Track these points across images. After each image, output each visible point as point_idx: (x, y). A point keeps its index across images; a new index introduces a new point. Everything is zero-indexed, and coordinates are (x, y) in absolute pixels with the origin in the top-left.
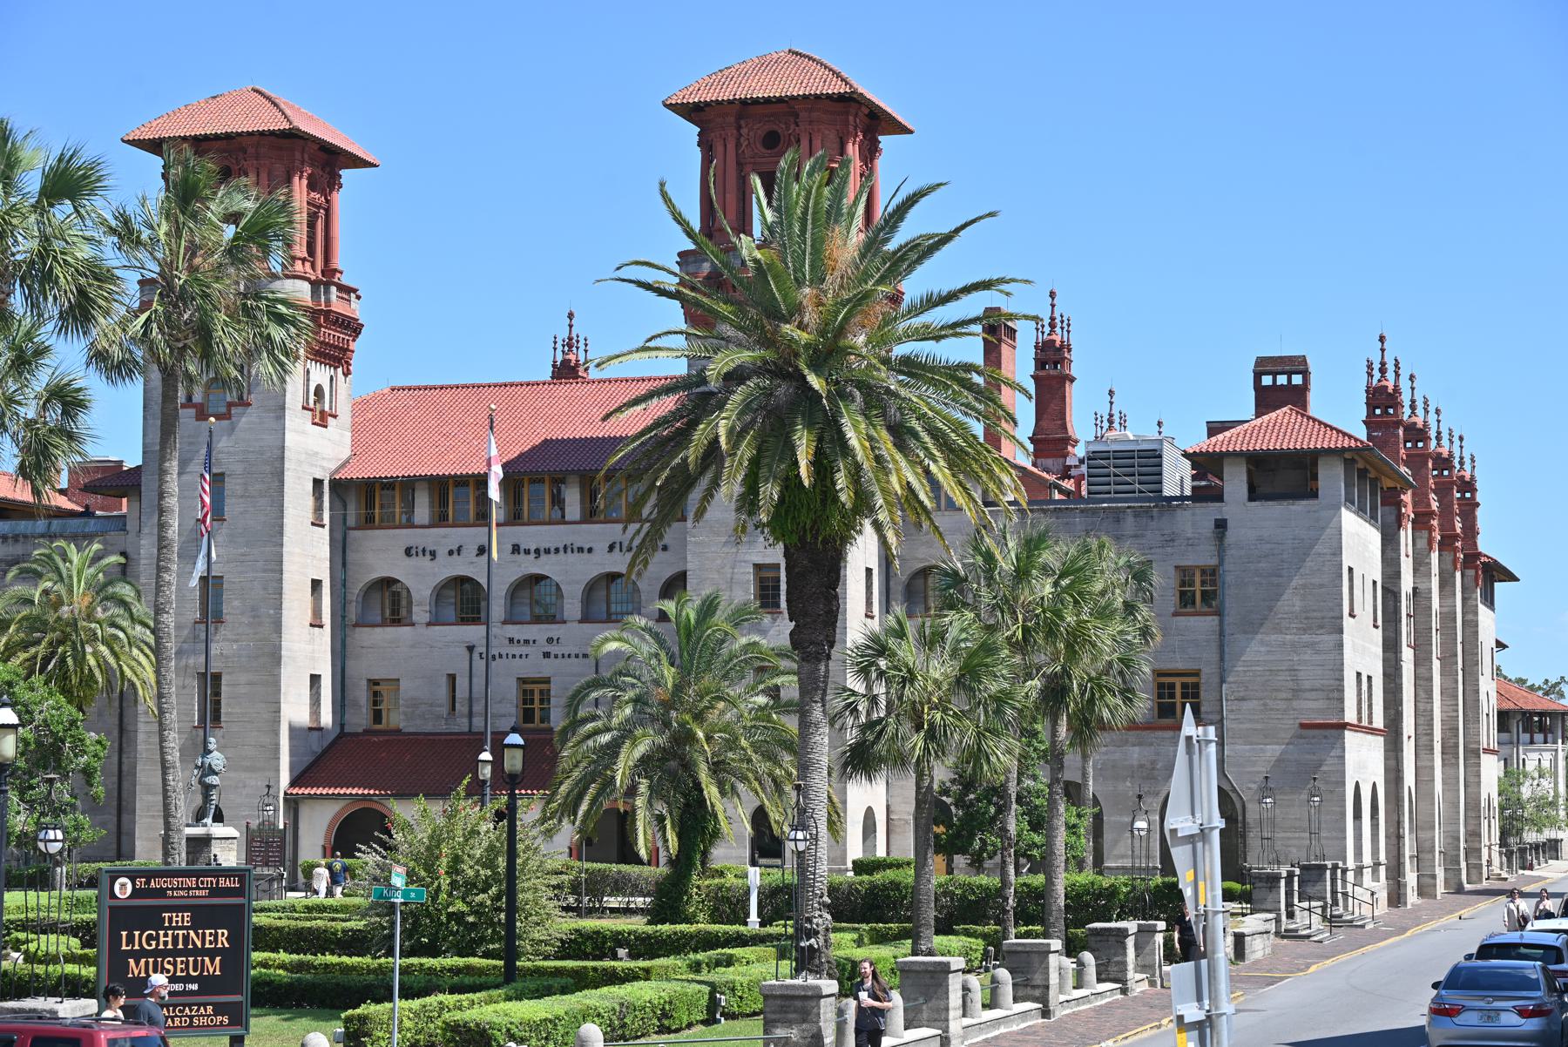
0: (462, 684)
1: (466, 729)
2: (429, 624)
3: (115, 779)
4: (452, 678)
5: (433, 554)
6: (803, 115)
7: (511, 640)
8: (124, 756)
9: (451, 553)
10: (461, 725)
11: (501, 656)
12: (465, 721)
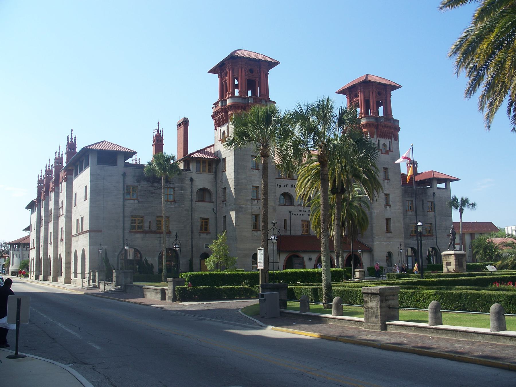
0: (288, 221)
1: (290, 234)
2: (279, 205)
3: (190, 247)
4: (285, 220)
5: (280, 186)
6: (388, 89)
7: (300, 210)
8: (193, 240)
9: (285, 186)
10: (288, 233)
11: (298, 215)
12: (290, 232)
